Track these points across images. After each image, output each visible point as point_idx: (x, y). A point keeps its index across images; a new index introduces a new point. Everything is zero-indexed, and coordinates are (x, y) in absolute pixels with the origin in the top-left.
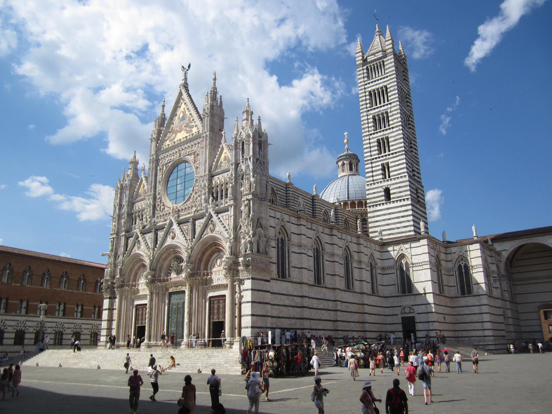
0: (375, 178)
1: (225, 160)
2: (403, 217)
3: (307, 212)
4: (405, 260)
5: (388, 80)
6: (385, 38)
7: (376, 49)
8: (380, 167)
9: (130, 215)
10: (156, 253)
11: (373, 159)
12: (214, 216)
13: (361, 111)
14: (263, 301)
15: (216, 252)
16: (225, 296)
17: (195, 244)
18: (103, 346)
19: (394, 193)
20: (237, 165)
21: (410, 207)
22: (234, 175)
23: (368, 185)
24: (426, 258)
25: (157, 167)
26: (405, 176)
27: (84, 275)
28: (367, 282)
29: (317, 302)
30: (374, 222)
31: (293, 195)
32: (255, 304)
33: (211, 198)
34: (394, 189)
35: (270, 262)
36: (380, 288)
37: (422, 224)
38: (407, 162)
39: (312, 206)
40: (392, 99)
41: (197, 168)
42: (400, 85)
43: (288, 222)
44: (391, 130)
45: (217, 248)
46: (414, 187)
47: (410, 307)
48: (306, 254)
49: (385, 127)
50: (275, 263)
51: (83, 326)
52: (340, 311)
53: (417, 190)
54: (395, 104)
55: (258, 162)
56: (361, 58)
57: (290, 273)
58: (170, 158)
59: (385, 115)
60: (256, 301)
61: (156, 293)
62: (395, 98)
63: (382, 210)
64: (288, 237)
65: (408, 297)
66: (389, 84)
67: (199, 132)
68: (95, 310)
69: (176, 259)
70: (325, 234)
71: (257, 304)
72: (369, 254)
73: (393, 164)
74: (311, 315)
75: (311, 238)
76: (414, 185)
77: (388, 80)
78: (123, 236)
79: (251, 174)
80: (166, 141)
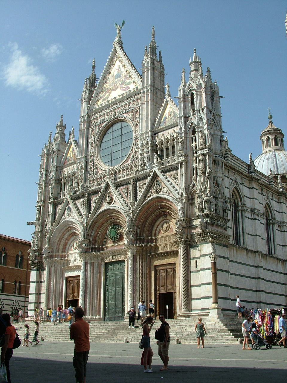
9: (59, 182)
10: (89, 221)
12: (160, 175)
15: (161, 216)
17: (137, 208)
18: (31, 320)
20: (186, 118)
22: (183, 129)
25: (88, 129)
27: (4, 248)
29: (270, 274)
43: (240, 184)
45: (164, 212)
48: (259, 220)
57: (245, 240)
67: (137, 88)
68: (16, 285)
69: (114, 225)
78: (51, 203)
79: (206, 126)
80: (98, 100)
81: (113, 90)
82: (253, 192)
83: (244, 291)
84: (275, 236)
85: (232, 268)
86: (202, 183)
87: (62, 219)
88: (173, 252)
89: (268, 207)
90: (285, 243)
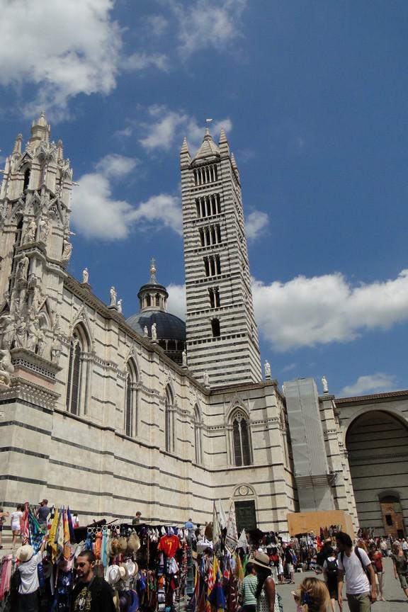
2: (236, 358)
8: (208, 293)
11: (197, 282)
19: (225, 327)
23: (189, 314)
26: (241, 305)
29: (125, 467)
30: (196, 364)
34: (225, 321)
43: (91, 320)
50: (64, 384)
52: (158, 485)
55: (53, 201)
57: (88, 408)
59: (215, 228)
62: (230, 209)
63: (207, 348)
64: (89, 345)
65: (246, 470)
66: (223, 192)
71: (23, 455)
72: (194, 404)
73: (225, 289)
82: (110, 336)
83: (75, 493)
85: (57, 451)
89: (132, 364)
90: (153, 420)
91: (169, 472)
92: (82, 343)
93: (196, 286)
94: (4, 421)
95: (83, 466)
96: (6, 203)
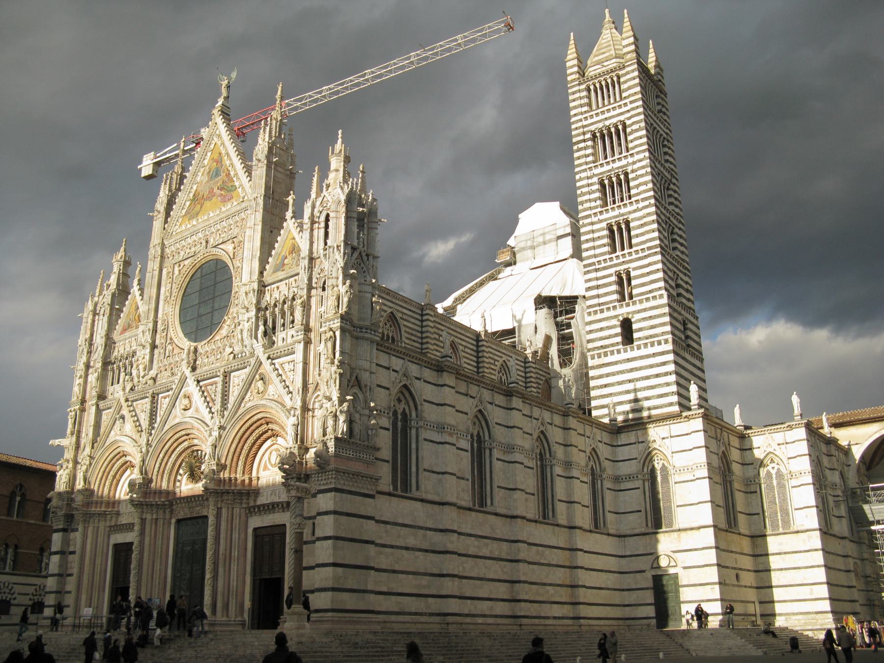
0: (602, 300)
1: (291, 253)
2: (657, 376)
3: (465, 365)
4: (661, 463)
5: (628, 111)
6: (621, 34)
7: (604, 53)
8: (614, 278)
12: (267, 366)
13: (577, 170)
14: (360, 538)
16: (284, 525)
19: (640, 330)
21: (671, 357)
24: (701, 456)
28: (583, 506)
29: (476, 543)
30: (602, 387)
31: (436, 331)
32: (341, 542)
33: (261, 328)
35: (376, 459)
36: (610, 517)
37: (694, 389)
38: (666, 269)
39: (475, 354)
40: (636, 147)
41: (239, 267)
42: (652, 121)
43: (417, 378)
44: (635, 207)
45: (272, 430)
46: (680, 318)
47: (668, 556)
48: (454, 445)
49: (622, 200)
50: (388, 462)
51: (17, 589)
52: (525, 561)
53: (684, 324)
54: (641, 156)
55: (356, 255)
56: (576, 69)
58: (188, 251)
59: (622, 177)
60: (343, 535)
61: (152, 519)
62: (641, 145)
63: (616, 363)
64: (416, 409)
66: (629, 118)
70: (496, 405)
72: (588, 450)
74: (464, 568)
75: (467, 414)
76: (680, 314)
77: (628, 111)
81: (206, 200)
83: (411, 577)
84: (493, 472)
86: (327, 382)
87: (110, 436)
88: (282, 503)
89: (481, 416)
91: (545, 543)
92: (409, 407)
93: (597, 270)
94: (324, 510)
95: (419, 547)
96: (307, 258)
